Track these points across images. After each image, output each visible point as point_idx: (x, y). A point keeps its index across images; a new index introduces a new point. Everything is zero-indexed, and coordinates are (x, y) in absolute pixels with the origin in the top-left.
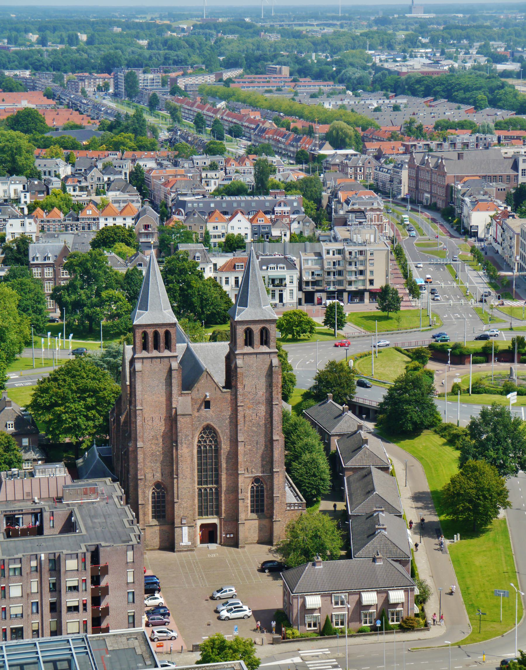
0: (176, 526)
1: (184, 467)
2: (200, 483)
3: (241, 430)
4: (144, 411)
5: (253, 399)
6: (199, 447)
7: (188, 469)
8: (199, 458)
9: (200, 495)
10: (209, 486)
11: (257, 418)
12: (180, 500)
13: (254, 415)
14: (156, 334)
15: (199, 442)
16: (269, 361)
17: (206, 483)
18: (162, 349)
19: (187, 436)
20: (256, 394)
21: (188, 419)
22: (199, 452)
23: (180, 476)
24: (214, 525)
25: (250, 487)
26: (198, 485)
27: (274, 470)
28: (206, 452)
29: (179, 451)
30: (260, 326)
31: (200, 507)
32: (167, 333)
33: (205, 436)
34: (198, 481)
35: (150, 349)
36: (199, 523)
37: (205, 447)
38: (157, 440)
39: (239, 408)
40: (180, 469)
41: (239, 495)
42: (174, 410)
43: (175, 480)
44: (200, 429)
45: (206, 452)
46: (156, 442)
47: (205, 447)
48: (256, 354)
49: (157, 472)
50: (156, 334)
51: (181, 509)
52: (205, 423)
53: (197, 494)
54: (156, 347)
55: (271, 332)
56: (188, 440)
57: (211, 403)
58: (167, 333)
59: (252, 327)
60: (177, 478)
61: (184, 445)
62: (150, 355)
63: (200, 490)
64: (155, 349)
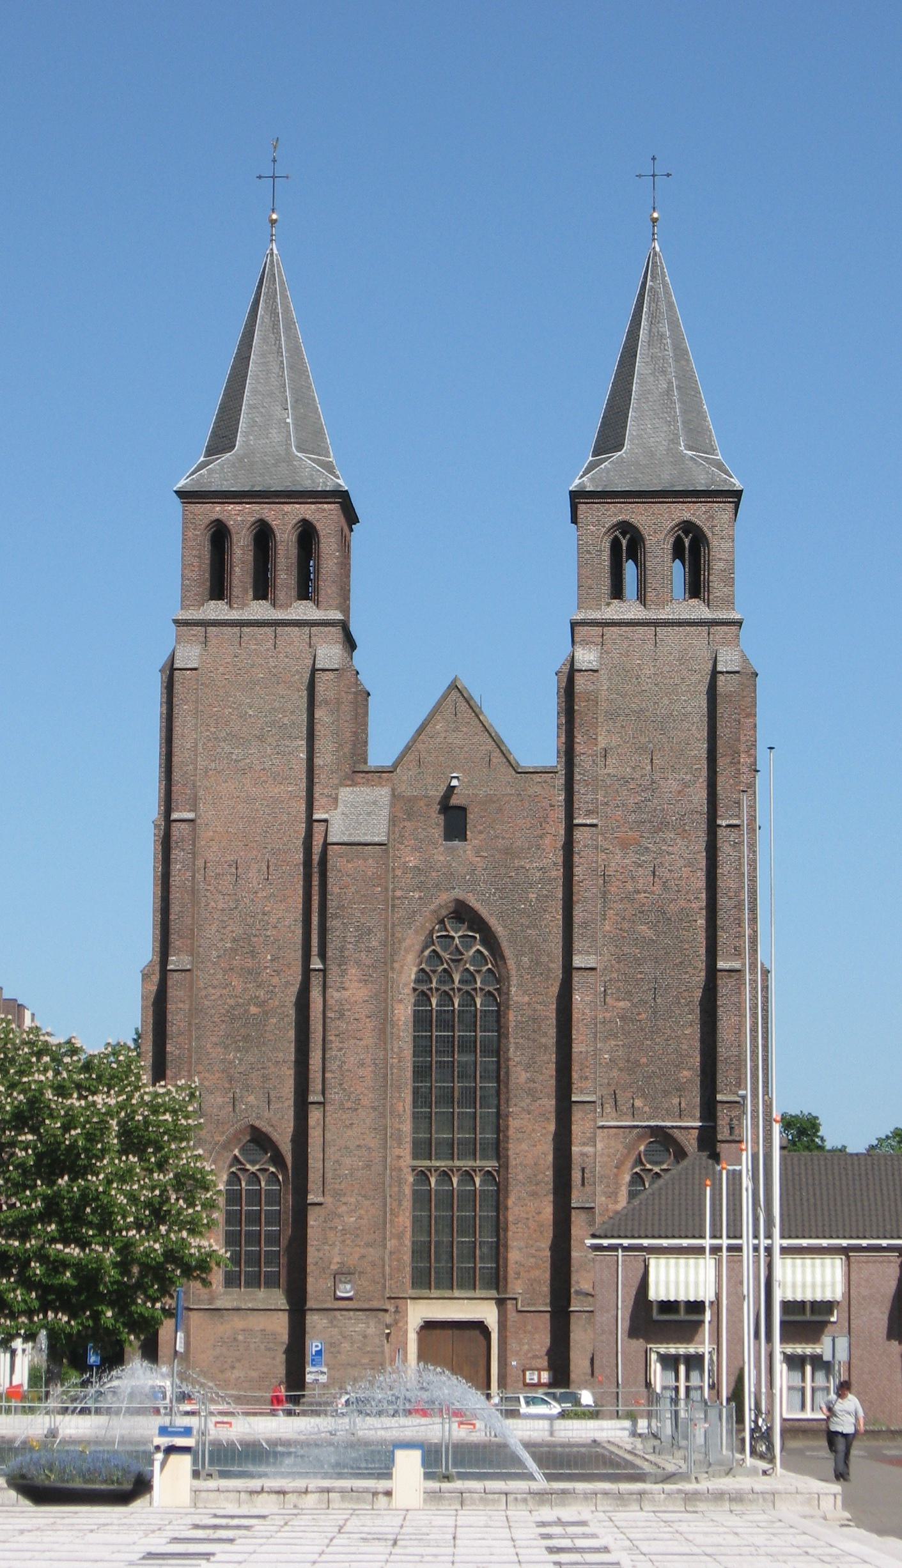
0: (310, 1304)
1: (352, 1060)
2: (422, 1149)
3: (585, 924)
4: (205, 834)
5: (638, 808)
6: (423, 997)
7: (367, 1072)
8: (421, 1047)
9: (421, 1199)
10: (457, 1163)
11: (657, 889)
12: (328, 1200)
13: (643, 876)
14: (263, 535)
15: (423, 976)
16: (708, 655)
17: (449, 1149)
18: (281, 595)
19: (365, 933)
20: (653, 786)
21: (369, 865)
22: (421, 1020)
23: (334, 1095)
24: (480, 1327)
25: (627, 1178)
26: (416, 1156)
27: (719, 1097)
28: (446, 1022)
29: (334, 994)
30: (669, 516)
31: (420, 1251)
32: (307, 535)
33: (446, 956)
34: (416, 1144)
35: (236, 591)
36: (418, 1313)
37: (447, 997)
38: (253, 954)
39: (578, 834)
40: (332, 1066)
41: (575, 1194)
42: (318, 829)
43: (314, 1116)
44: (425, 920)
45: (446, 1022)
46: (249, 963)
47: (447, 997)
48: (656, 624)
49: (247, 1087)
50: (263, 535)
51: (331, 1234)
52: (445, 898)
53: (408, 1191)
54: (263, 589)
55: (714, 542)
56: (369, 950)
57: (471, 817)
58: (307, 535)
59: (639, 515)
60: (323, 1104)
61: (353, 971)
62: (234, 615)
63: (422, 1176)
64: (257, 597)
